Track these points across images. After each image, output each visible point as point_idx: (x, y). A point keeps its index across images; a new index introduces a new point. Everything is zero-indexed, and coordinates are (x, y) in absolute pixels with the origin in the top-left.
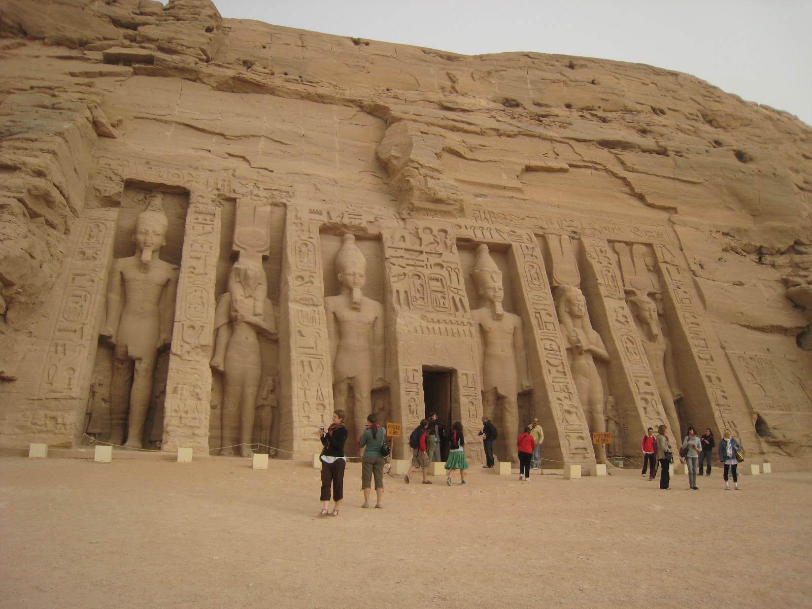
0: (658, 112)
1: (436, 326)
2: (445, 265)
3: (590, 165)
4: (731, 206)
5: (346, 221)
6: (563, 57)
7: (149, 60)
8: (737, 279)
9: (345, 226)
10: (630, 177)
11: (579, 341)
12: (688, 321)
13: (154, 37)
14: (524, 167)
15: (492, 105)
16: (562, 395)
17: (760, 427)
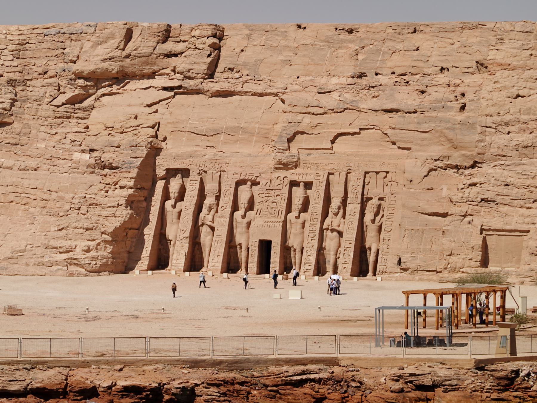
0: (446, 70)
1: (266, 224)
2: (281, 195)
3: (372, 127)
4: (443, 143)
5: (246, 178)
6: (412, 24)
7: (180, 87)
8: (430, 187)
9: (246, 180)
10: (389, 132)
11: (329, 226)
12: (389, 212)
13: (182, 71)
14: (335, 134)
15: (350, 80)
16: (309, 249)
17: (400, 262)
